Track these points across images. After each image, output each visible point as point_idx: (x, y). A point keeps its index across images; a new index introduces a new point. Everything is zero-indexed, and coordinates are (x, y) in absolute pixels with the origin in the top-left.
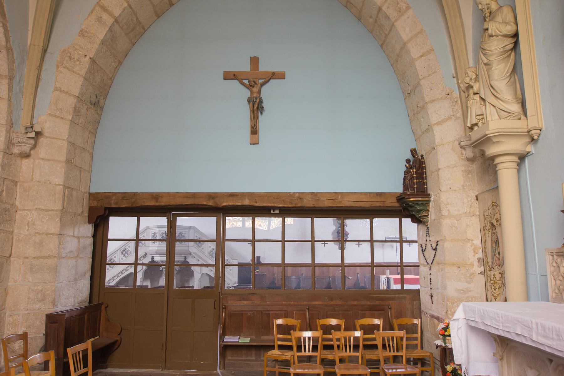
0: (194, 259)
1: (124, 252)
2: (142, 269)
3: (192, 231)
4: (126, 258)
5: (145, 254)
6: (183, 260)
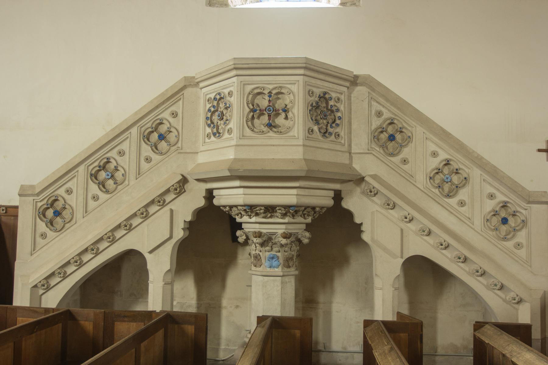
0: (374, 199)
1: (103, 175)
2: (171, 237)
3: (360, 91)
4: (107, 196)
5: (178, 182)
6: (330, 202)
